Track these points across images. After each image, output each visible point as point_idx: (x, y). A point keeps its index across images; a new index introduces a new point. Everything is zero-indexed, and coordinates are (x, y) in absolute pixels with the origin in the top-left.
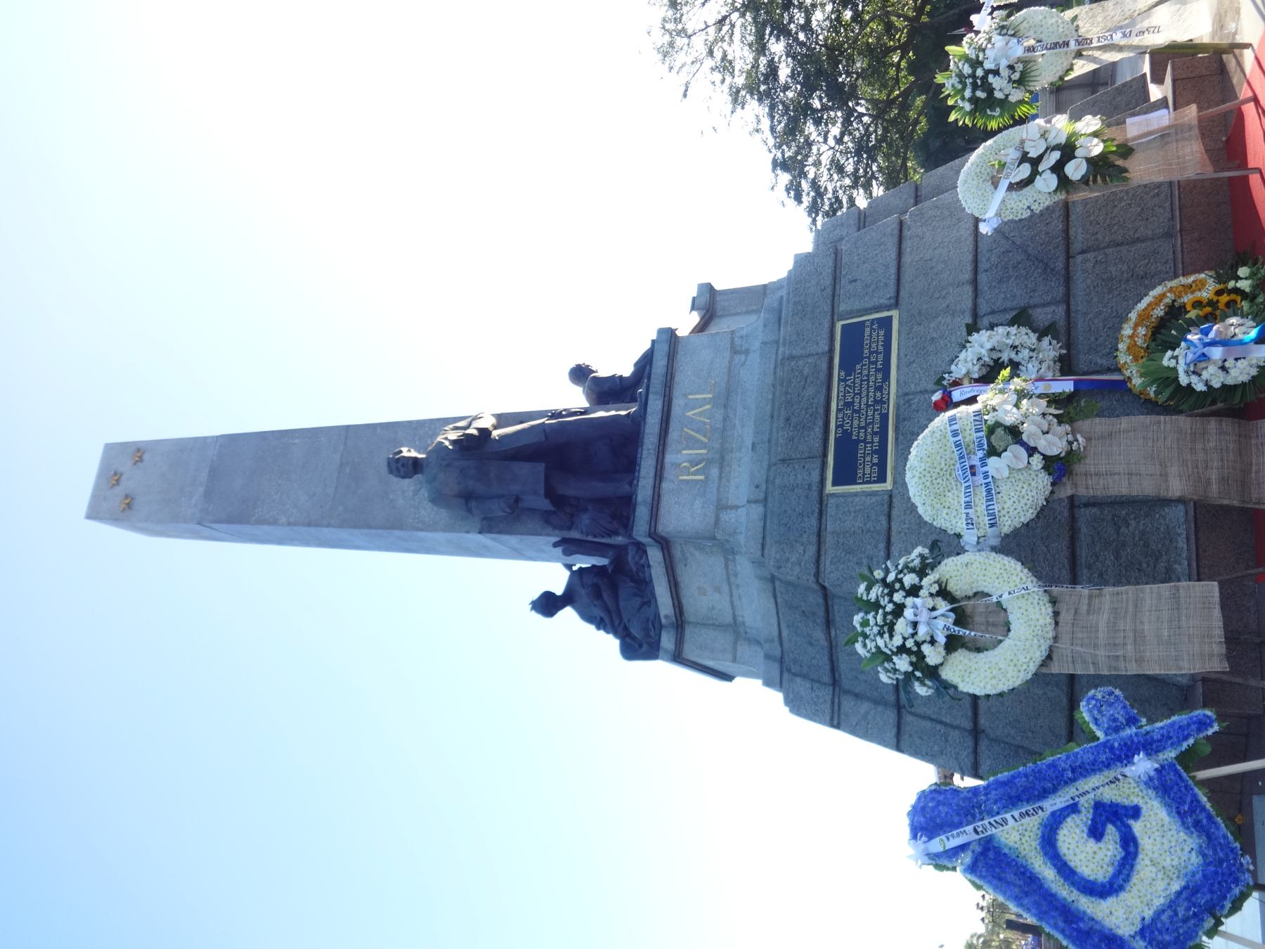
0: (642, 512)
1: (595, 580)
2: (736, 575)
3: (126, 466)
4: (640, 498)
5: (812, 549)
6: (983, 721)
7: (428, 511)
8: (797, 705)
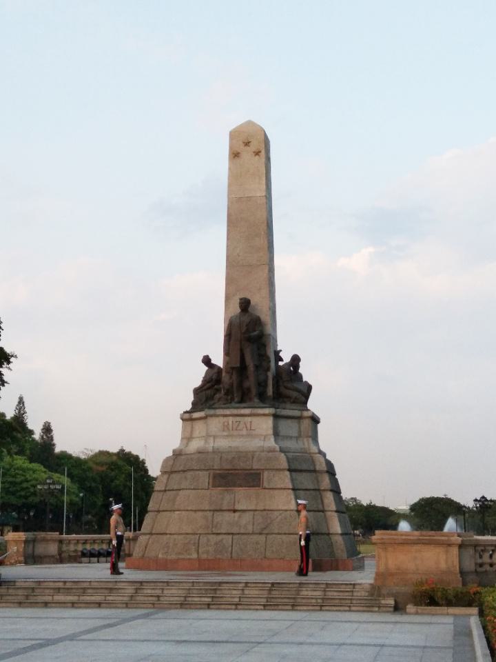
0: (212, 412)
3: (254, 146)
5: (195, 468)
7: (230, 316)
8: (167, 460)
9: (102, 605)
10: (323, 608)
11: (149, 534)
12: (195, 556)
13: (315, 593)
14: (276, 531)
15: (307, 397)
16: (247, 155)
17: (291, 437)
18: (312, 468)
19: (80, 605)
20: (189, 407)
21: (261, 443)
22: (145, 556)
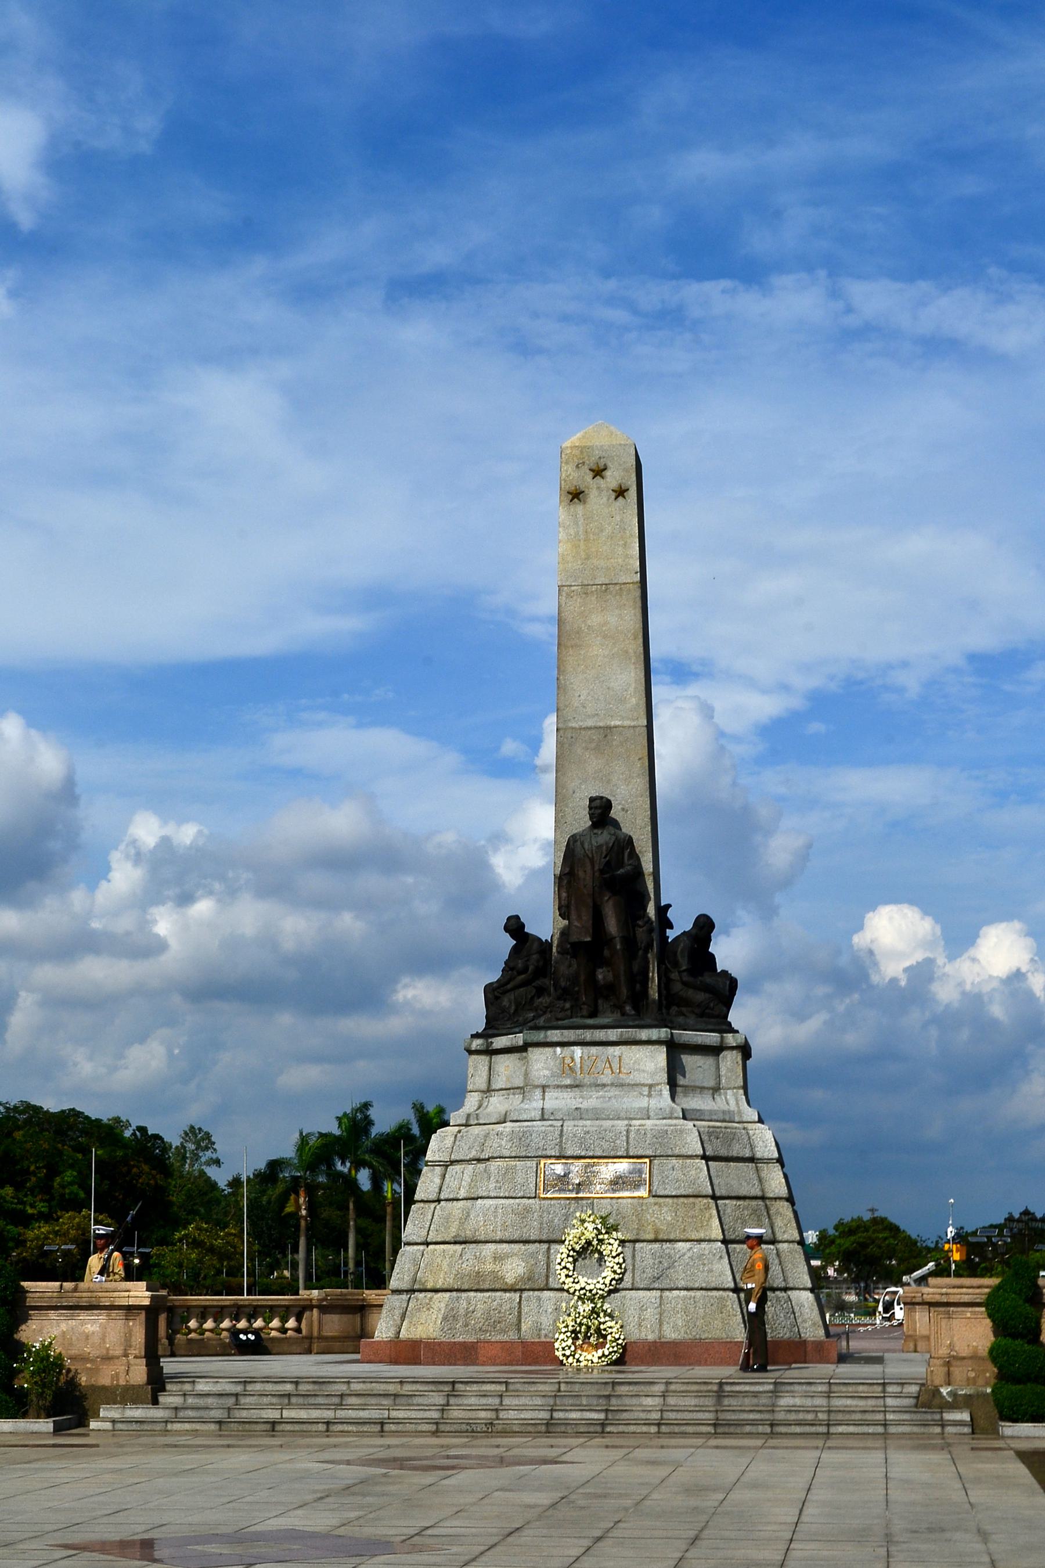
0: (540, 1036)
1: (531, 968)
2: (514, 1094)
3: (613, 478)
4: (549, 1032)
5: (507, 1153)
6: (431, 1247)
9: (387, 1428)
10: (833, 1430)
11: (407, 1291)
12: (512, 1336)
13: (808, 1402)
14: (682, 1284)
15: (727, 1001)
16: (598, 497)
17: (702, 1088)
18: (747, 1154)
19: (340, 1427)
20: (481, 1027)
21: (643, 1102)
22: (403, 1335)
